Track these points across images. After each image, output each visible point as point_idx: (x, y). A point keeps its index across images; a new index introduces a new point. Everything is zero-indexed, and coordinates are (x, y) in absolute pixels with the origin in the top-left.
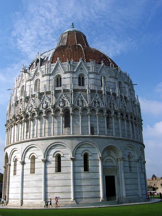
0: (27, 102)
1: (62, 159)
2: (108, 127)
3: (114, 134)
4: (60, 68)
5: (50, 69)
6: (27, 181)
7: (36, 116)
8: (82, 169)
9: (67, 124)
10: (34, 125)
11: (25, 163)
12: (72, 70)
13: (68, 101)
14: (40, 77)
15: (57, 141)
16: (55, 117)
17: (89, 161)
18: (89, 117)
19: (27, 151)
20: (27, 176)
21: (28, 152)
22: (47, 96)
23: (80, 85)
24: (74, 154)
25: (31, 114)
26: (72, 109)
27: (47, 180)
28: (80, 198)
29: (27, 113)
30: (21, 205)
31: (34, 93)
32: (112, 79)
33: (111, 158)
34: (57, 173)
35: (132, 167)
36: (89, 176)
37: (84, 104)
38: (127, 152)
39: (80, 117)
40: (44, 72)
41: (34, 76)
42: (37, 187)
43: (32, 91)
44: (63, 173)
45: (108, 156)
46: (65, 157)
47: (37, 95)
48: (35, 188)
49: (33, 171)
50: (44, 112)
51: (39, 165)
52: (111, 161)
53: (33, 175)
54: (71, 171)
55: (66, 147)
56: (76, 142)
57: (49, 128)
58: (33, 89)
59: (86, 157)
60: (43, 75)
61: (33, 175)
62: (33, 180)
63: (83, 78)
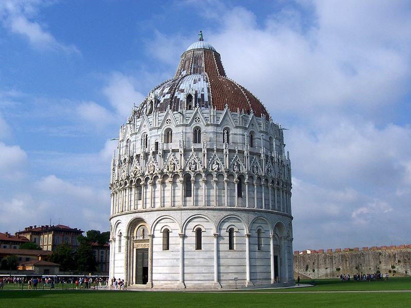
8: (257, 247)
10: (197, 189)
15: (232, 213)
19: (189, 222)
21: (190, 223)
24: (250, 230)
25: (194, 174)
28: (255, 279)
30: (185, 287)
36: (262, 255)
39: (255, 187)
48: (204, 267)
54: (246, 249)
55: (241, 221)
56: (252, 217)
58: (192, 139)
62: (201, 257)
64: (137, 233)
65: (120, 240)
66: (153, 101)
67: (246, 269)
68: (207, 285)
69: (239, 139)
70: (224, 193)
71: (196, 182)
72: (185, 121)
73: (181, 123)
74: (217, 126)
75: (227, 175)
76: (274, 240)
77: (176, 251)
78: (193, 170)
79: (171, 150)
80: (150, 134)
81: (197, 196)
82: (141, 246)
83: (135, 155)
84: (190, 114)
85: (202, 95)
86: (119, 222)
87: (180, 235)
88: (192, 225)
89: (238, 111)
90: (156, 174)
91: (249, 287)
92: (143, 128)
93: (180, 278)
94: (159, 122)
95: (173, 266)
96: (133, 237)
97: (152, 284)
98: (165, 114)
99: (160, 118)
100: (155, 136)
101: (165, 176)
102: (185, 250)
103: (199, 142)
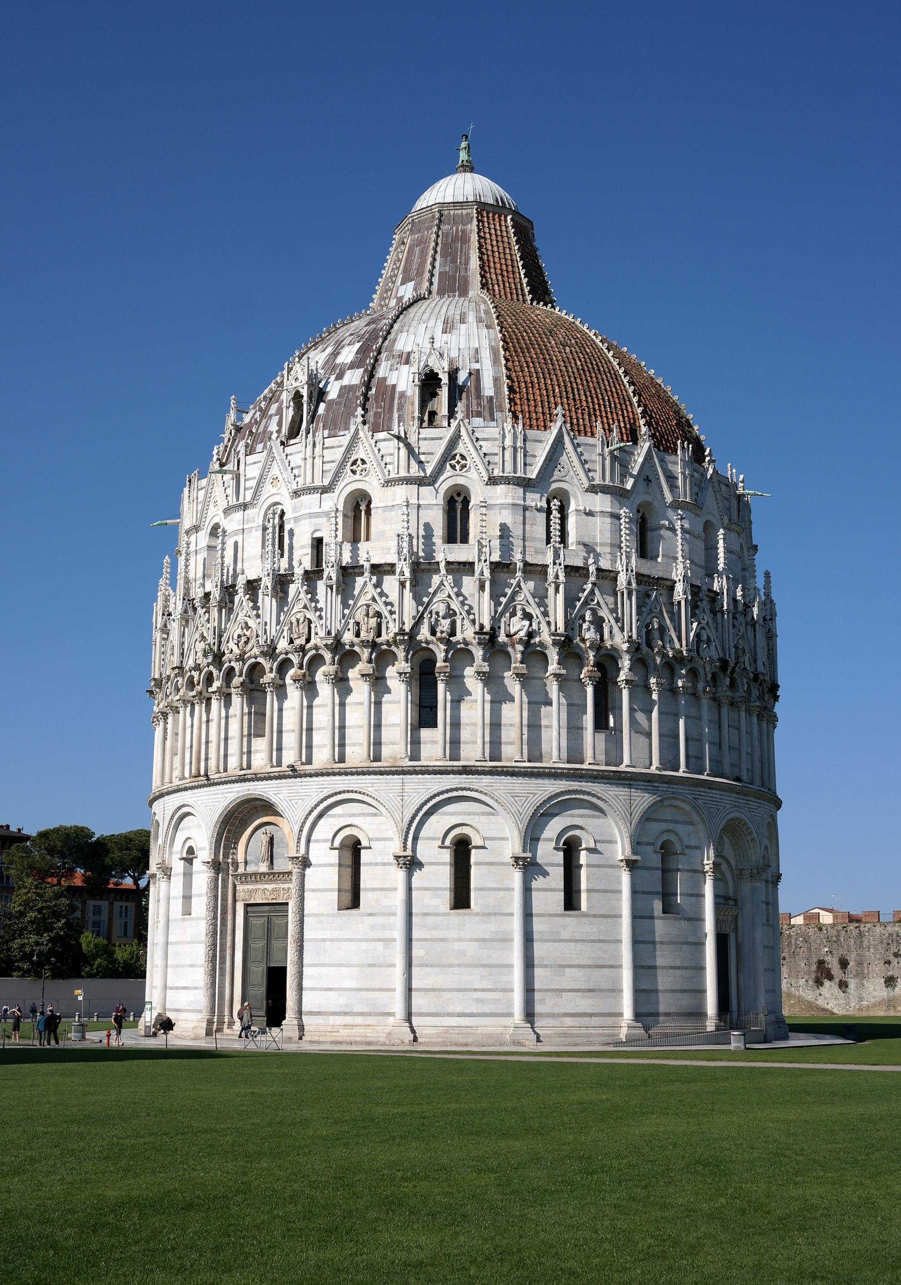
5: (525, 455)
10: (457, 702)
11: (420, 865)
19: (429, 813)
20: (429, 920)
24: (637, 844)
25: (447, 651)
30: (415, 1039)
39: (655, 696)
40: (498, 459)
53: (465, 914)
54: (620, 908)
56: (643, 800)
58: (439, 531)
60: (490, 479)
61: (466, 918)
64: (249, 849)
65: (188, 875)
66: (304, 392)
67: (621, 979)
68: (486, 1030)
69: (600, 531)
70: (549, 716)
71: (455, 680)
72: (414, 465)
73: (403, 474)
74: (526, 484)
75: (559, 654)
76: (716, 880)
77: (383, 914)
78: (444, 635)
79: (367, 566)
80: (295, 510)
81: (456, 725)
82: (263, 892)
83: (241, 581)
84: (432, 443)
85: (475, 375)
86: (184, 810)
87: (397, 857)
88: (437, 825)
89: (599, 430)
90: (316, 648)
91: (630, 1041)
92: (268, 489)
93: (398, 1008)
94: (327, 467)
95: (370, 965)
96: (236, 865)
97: (301, 1027)
98: (345, 439)
99: (329, 455)
100: (312, 515)
101: (346, 657)
102: (415, 910)
103: (465, 540)
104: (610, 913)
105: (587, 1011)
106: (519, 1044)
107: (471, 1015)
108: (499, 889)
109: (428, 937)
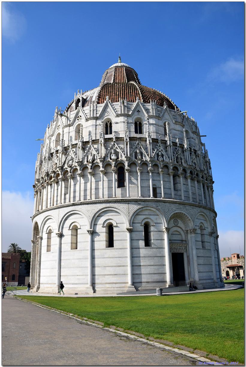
0: (65, 154)
1: (115, 229)
2: (175, 189)
3: (183, 198)
4: (110, 109)
5: (96, 111)
6: (67, 259)
7: (79, 172)
8: (142, 243)
9: (121, 183)
10: (75, 185)
11: (64, 236)
12: (126, 112)
13: (123, 152)
14: (82, 121)
16: (105, 173)
17: (152, 233)
18: (150, 174)
19: (66, 220)
22: (93, 146)
23: (136, 132)
24: (132, 222)
25: (71, 170)
26: (128, 163)
27: (95, 258)
29: (66, 169)
31: (74, 142)
32: (178, 126)
33: (179, 229)
34: (108, 249)
35: (205, 242)
37: (144, 157)
38: (199, 222)
39: (139, 174)
40: (89, 114)
41: (74, 121)
42: (81, 267)
43: (71, 140)
44: (117, 249)
45: (175, 226)
46: (119, 227)
47: (80, 144)
49: (75, 246)
50: (89, 167)
51: (84, 238)
52: (178, 233)
54: (127, 246)
56: (134, 208)
57: (97, 189)
59: (147, 227)
60: (86, 119)
63: (140, 124)
67: (127, 270)
95: (52, 268)
104: (123, 248)
105: (115, 282)
106: (88, 294)
107: (76, 284)
108: (85, 242)
109: (65, 259)
